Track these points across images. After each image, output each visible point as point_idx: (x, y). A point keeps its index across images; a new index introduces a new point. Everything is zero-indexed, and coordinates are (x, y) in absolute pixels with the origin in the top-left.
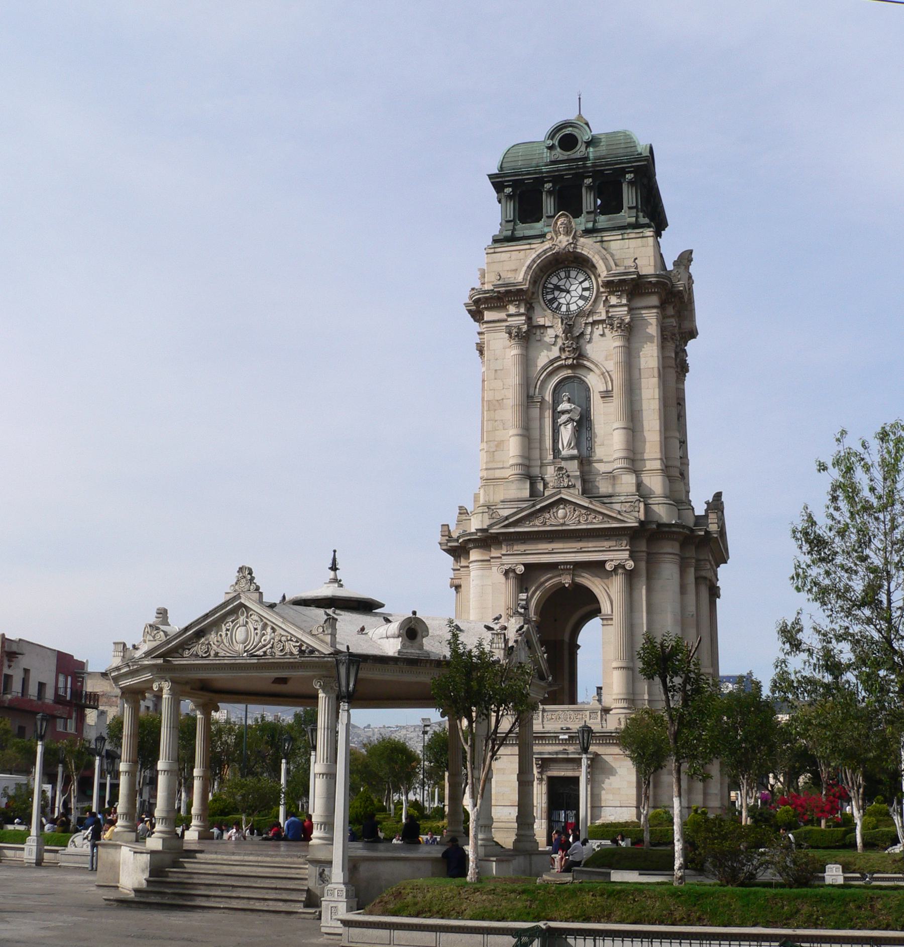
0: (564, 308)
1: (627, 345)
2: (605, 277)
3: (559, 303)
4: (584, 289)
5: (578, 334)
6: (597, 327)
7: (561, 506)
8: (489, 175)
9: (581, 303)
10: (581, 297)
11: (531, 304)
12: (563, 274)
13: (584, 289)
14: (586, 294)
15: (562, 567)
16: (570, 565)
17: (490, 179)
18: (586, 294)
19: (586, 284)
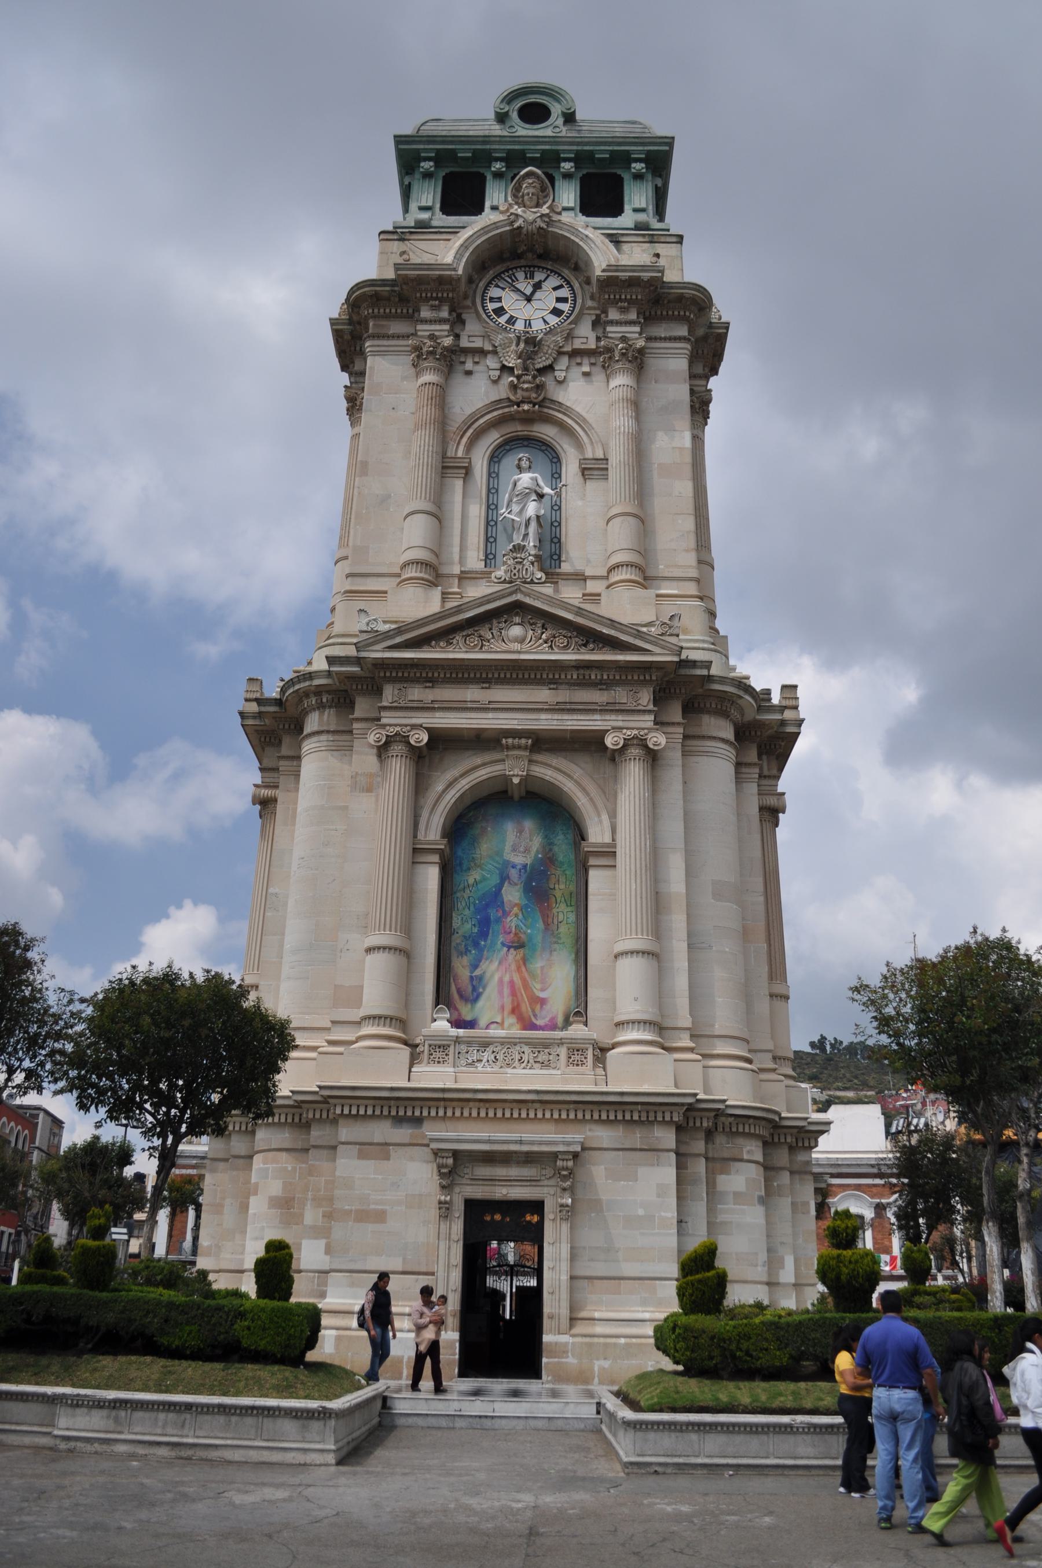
0: (520, 326)
1: (635, 386)
2: (604, 271)
3: (512, 317)
4: (559, 300)
5: (541, 366)
6: (579, 360)
7: (517, 619)
8: (330, 319)
9: (553, 320)
10: (556, 312)
11: (459, 316)
12: (520, 275)
13: (559, 300)
14: (565, 307)
15: (510, 740)
16: (528, 738)
17: (332, 324)
18: (565, 307)
19: (565, 293)
